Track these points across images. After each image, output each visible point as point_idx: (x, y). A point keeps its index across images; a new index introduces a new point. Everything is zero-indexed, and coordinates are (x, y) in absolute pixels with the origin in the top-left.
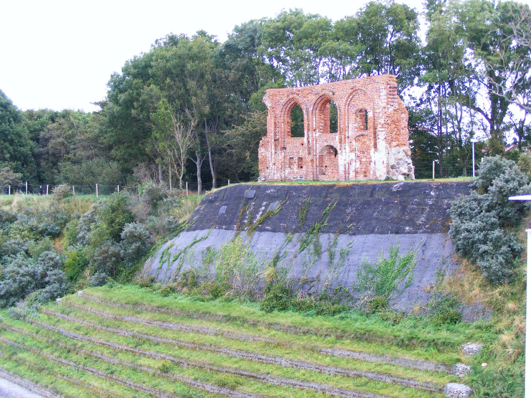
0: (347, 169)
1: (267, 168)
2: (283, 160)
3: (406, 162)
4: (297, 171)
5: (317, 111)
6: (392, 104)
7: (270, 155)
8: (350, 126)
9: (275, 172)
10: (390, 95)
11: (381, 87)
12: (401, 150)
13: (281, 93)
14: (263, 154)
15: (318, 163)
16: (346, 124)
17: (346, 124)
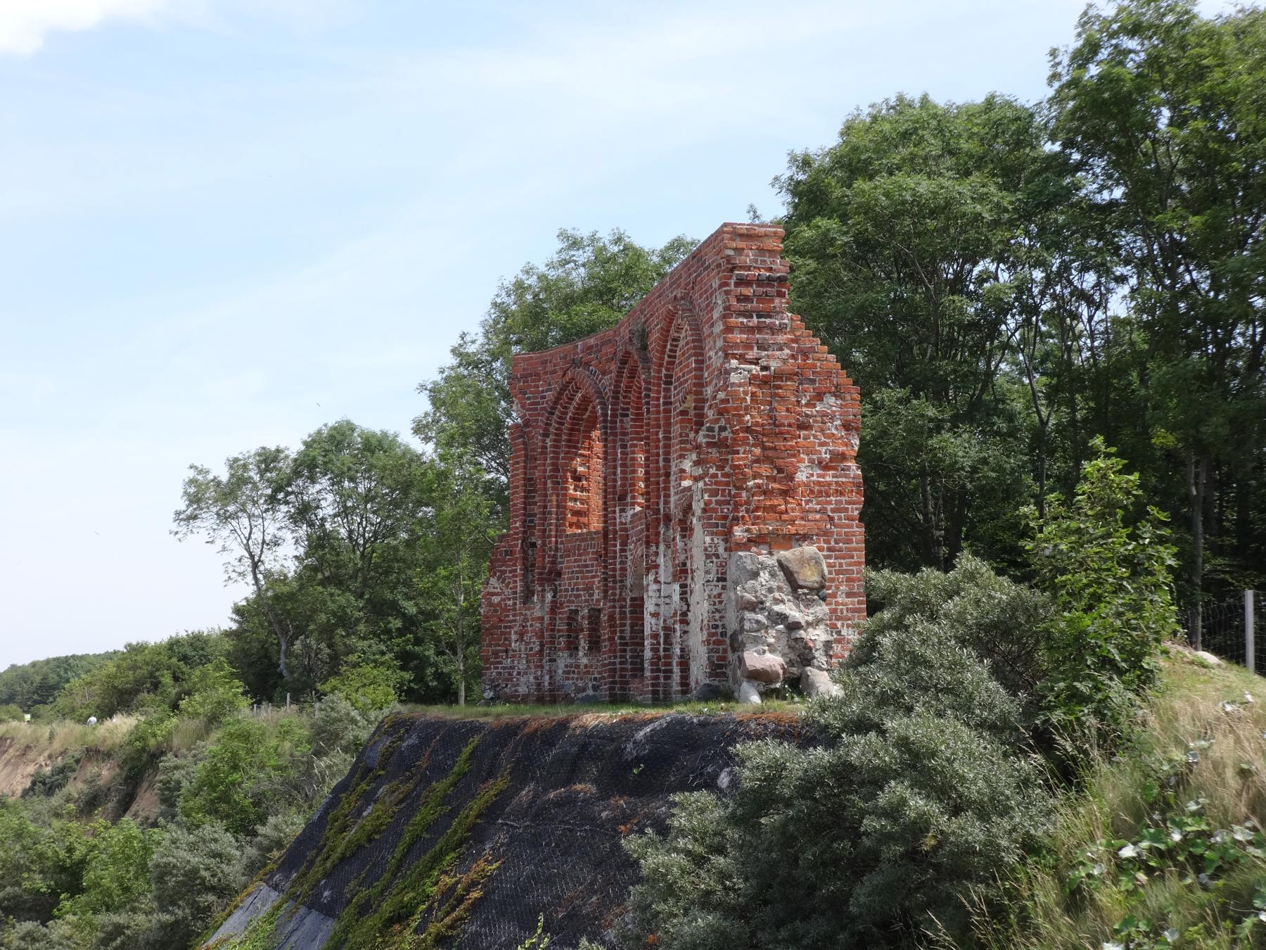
0: (662, 653)
1: (507, 651)
2: (546, 621)
3: (782, 618)
4: (585, 661)
5: (628, 422)
6: (751, 355)
7: (511, 603)
8: (673, 469)
9: (522, 665)
10: (748, 315)
11: (714, 285)
12: (771, 561)
13: (549, 367)
14: (496, 599)
15: (628, 628)
16: (661, 464)
17: (661, 464)
